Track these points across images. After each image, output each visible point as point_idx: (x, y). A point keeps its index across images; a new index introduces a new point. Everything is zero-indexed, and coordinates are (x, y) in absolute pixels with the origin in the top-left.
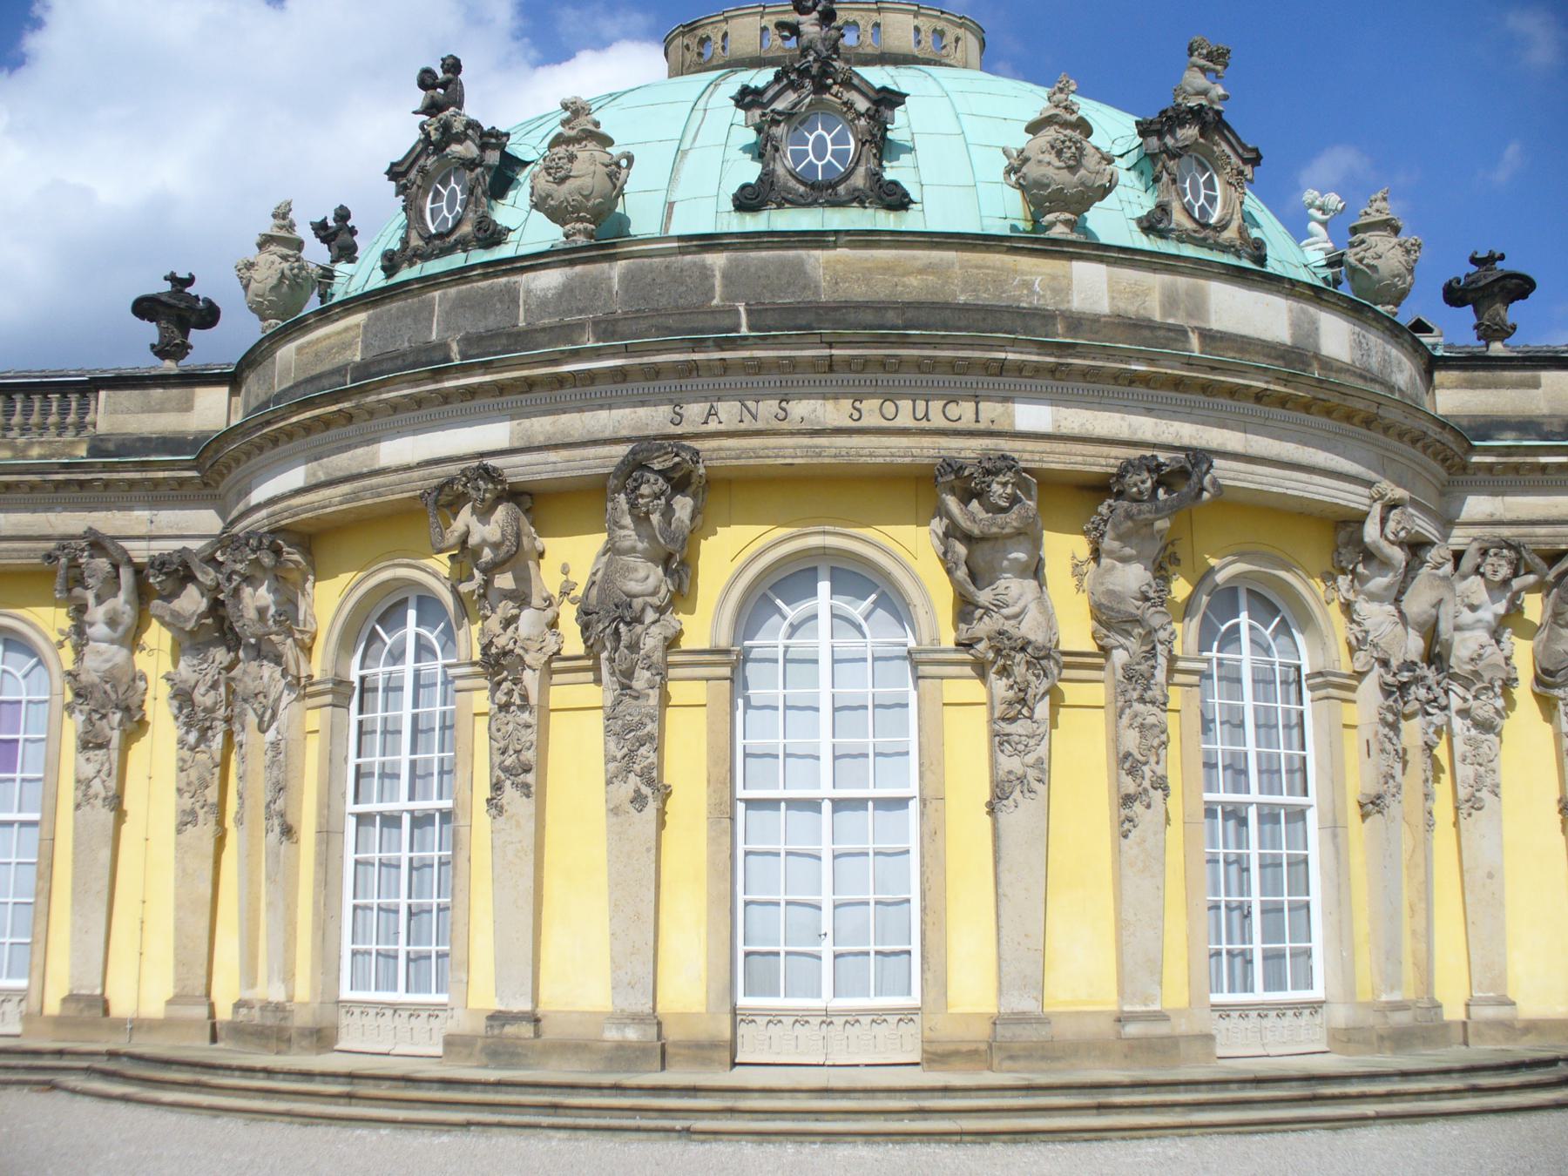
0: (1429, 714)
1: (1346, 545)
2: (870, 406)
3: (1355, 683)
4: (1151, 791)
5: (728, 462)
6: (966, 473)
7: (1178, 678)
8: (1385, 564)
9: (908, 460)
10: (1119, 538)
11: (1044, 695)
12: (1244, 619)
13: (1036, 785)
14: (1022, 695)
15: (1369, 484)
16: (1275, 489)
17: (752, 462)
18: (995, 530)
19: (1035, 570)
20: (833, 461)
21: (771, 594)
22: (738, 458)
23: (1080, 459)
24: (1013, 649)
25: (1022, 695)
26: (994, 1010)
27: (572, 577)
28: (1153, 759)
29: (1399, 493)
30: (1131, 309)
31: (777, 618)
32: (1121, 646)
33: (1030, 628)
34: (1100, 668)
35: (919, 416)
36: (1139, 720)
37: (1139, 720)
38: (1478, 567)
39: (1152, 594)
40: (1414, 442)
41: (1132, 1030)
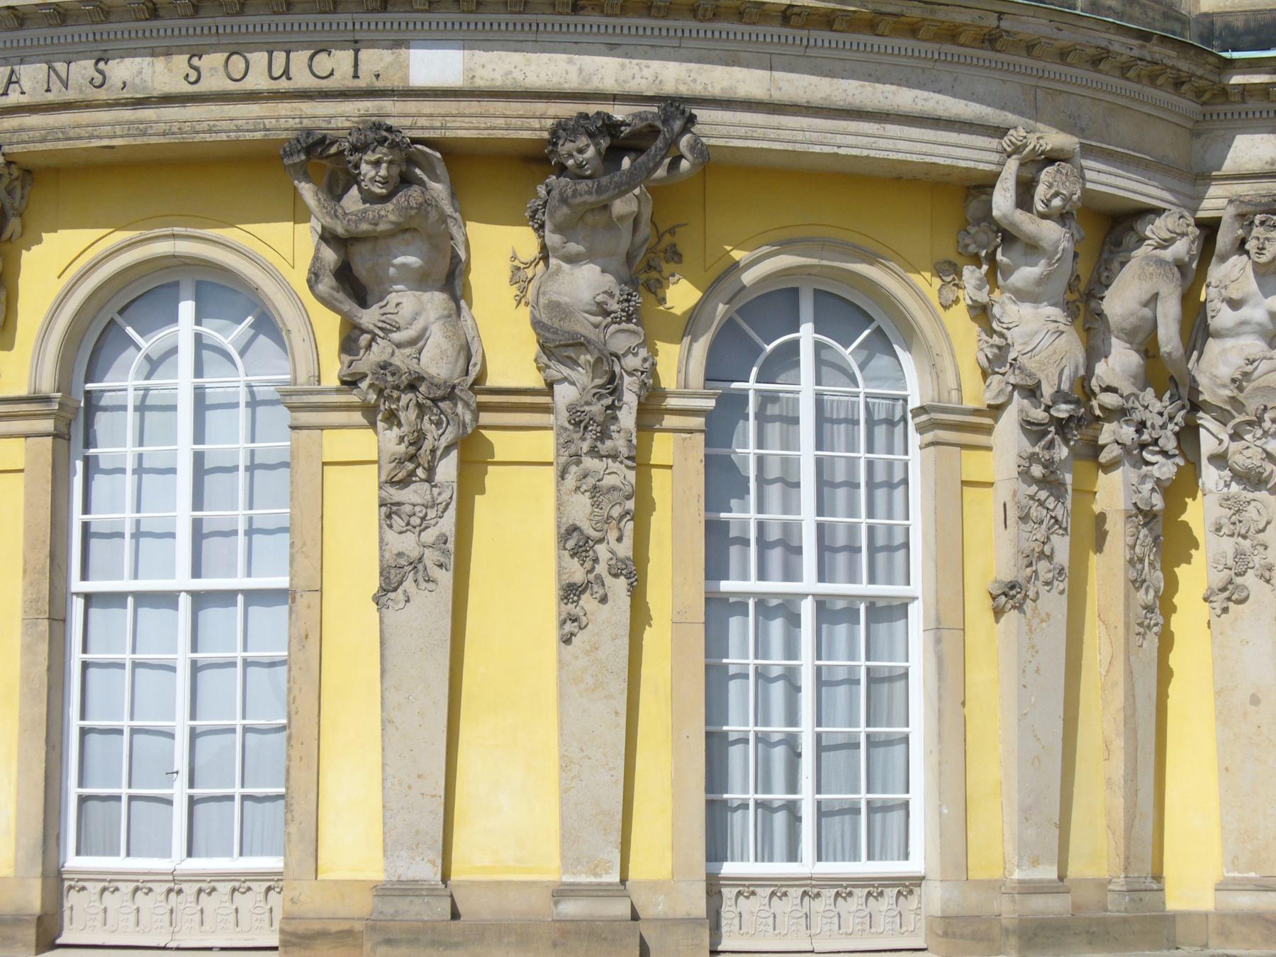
0: (1148, 463)
1: (977, 222)
2: (211, 61)
3: (988, 421)
4: (609, 580)
5: (31, 147)
6: (333, 150)
7: (669, 421)
8: (1033, 248)
9: (258, 135)
10: (558, 229)
11: (448, 449)
12: (806, 334)
13: (435, 572)
14: (412, 450)
15: (999, 131)
16: (817, 149)
17: (61, 145)
18: (364, 227)
19: (451, 278)
20: (162, 140)
21: (119, 319)
22: (43, 140)
23: (501, 122)
24: (397, 388)
25: (412, 450)
26: (380, 876)
28: (612, 536)
29: (1054, 139)
31: (132, 350)
32: (565, 379)
33: (436, 361)
34: (547, 409)
35: (276, 73)
36: (591, 481)
37: (591, 481)
38: (1243, 242)
39: (614, 306)
40: (1095, 62)
41: (570, 908)
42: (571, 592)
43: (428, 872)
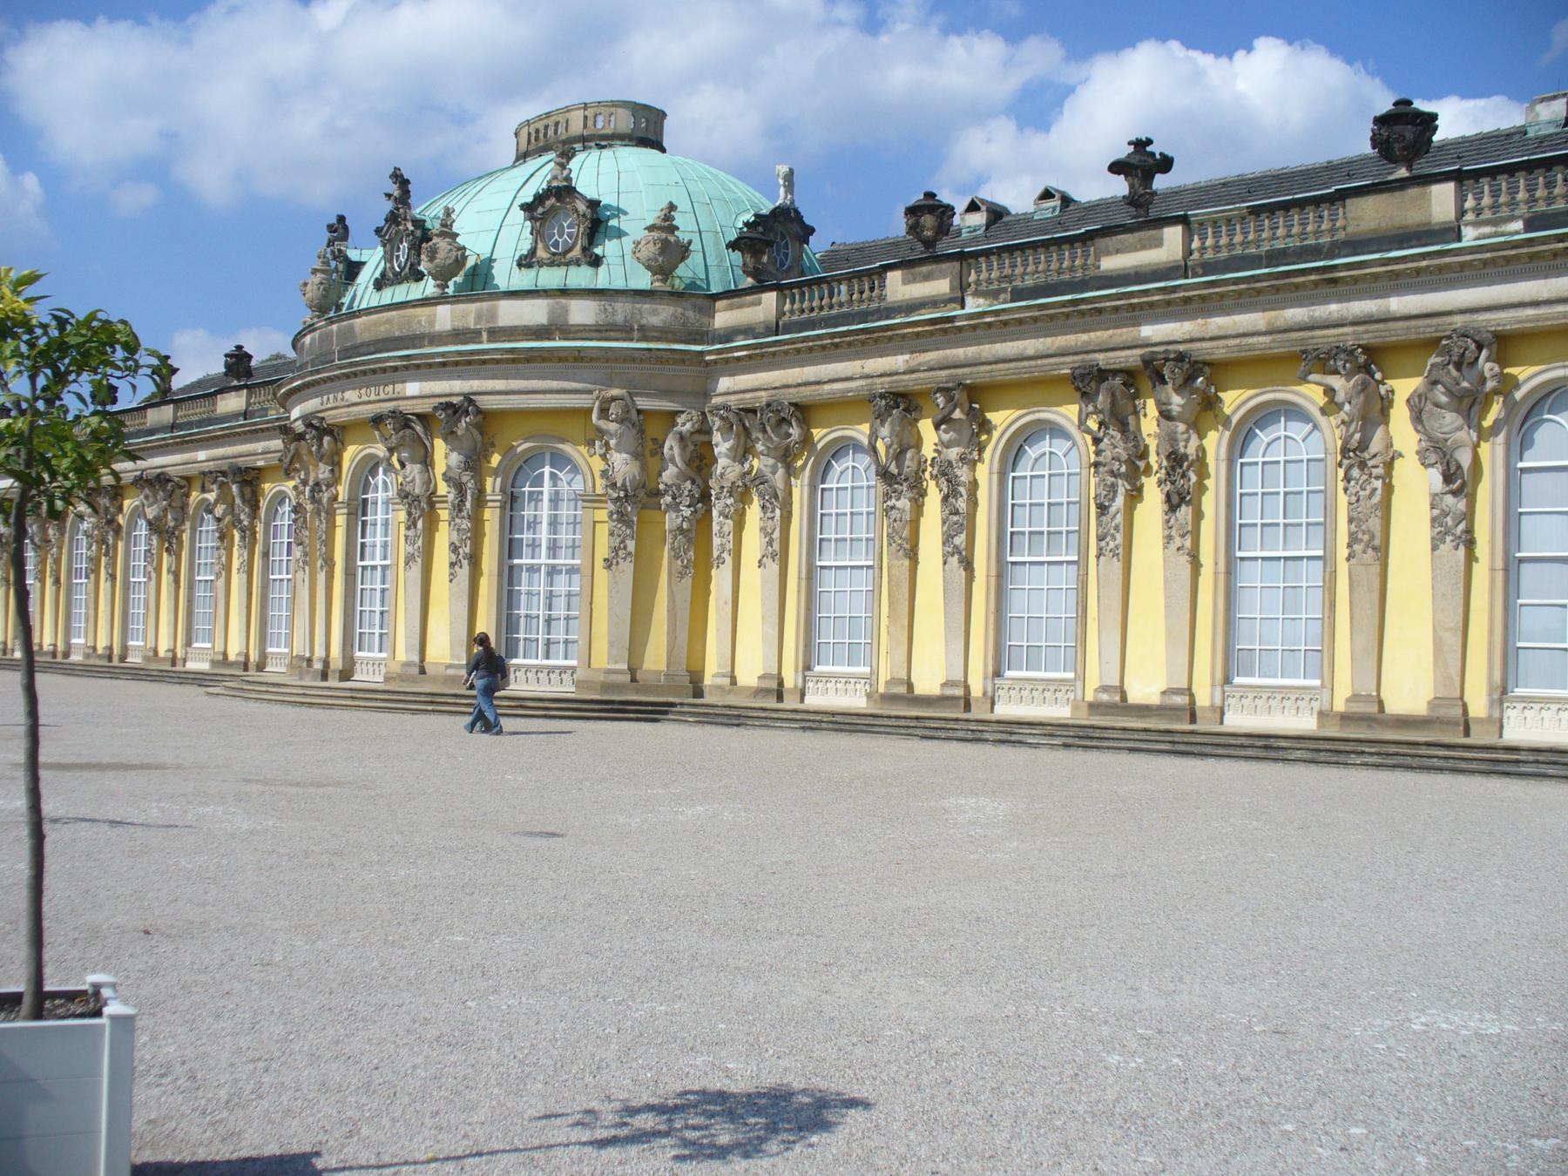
12: (547, 470)
30: (460, 324)
42: (452, 565)
43: (416, 659)
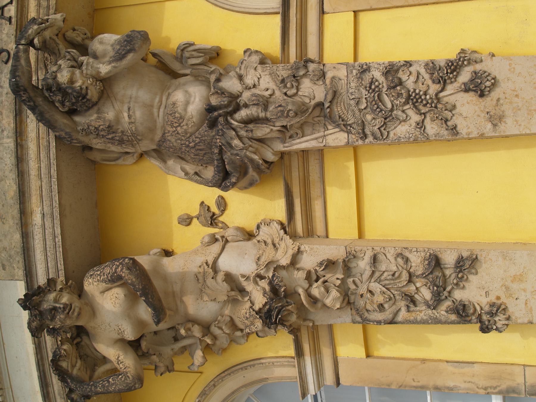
27: (195, 210)
